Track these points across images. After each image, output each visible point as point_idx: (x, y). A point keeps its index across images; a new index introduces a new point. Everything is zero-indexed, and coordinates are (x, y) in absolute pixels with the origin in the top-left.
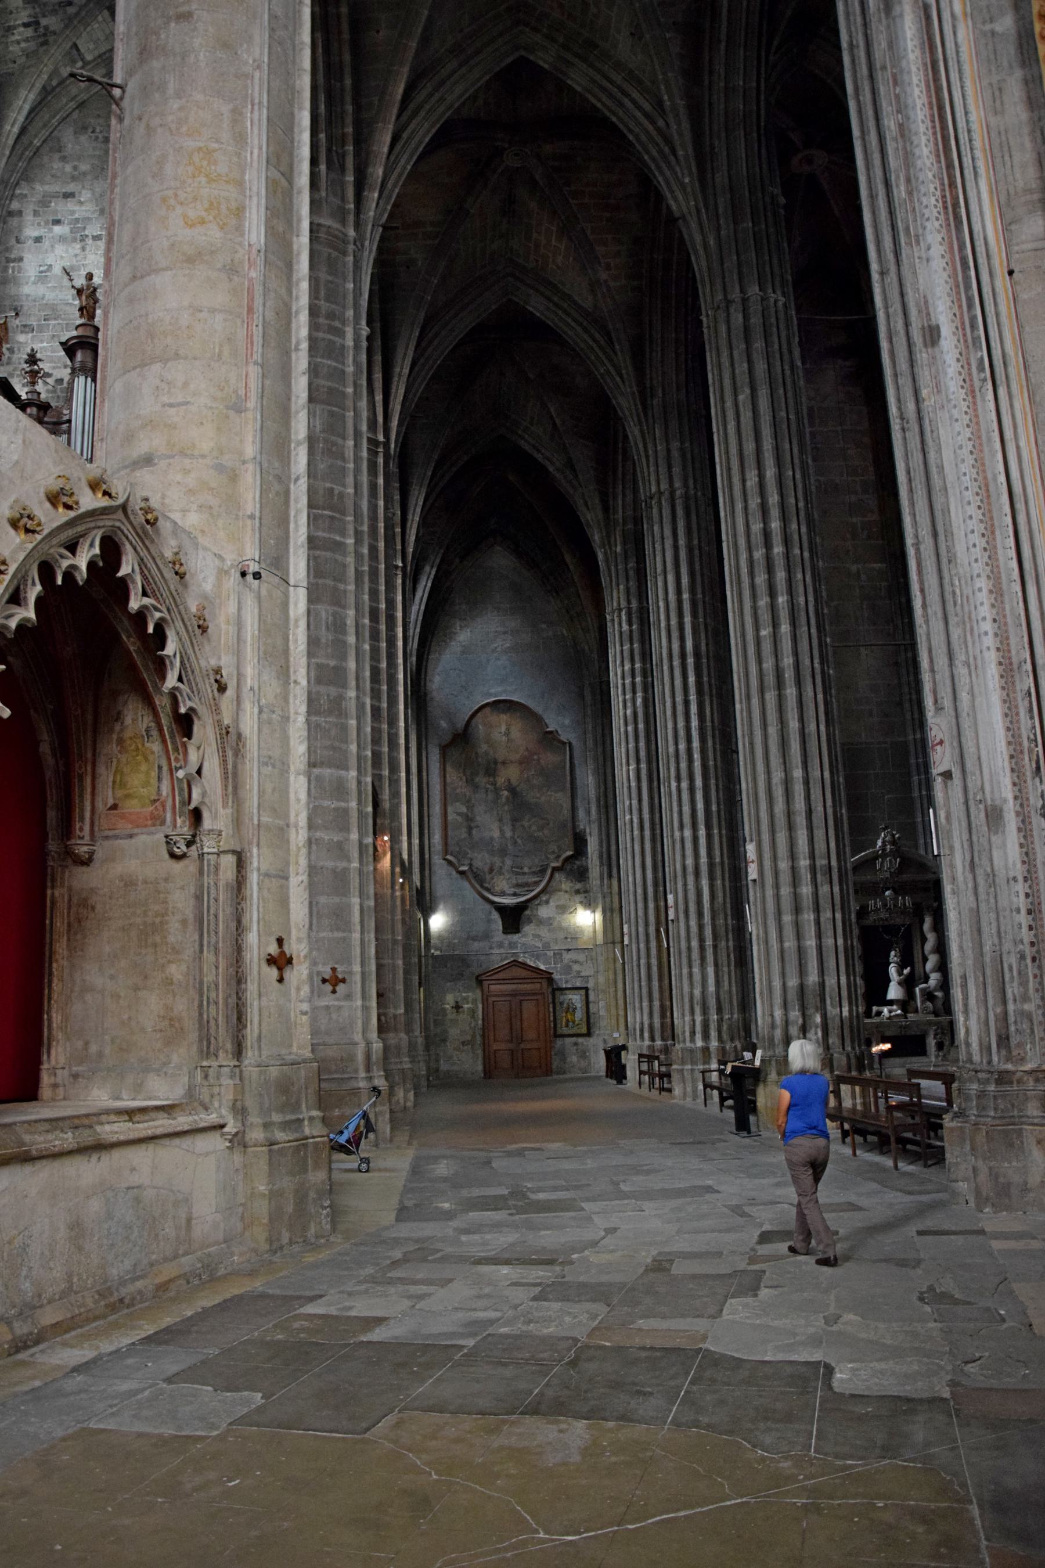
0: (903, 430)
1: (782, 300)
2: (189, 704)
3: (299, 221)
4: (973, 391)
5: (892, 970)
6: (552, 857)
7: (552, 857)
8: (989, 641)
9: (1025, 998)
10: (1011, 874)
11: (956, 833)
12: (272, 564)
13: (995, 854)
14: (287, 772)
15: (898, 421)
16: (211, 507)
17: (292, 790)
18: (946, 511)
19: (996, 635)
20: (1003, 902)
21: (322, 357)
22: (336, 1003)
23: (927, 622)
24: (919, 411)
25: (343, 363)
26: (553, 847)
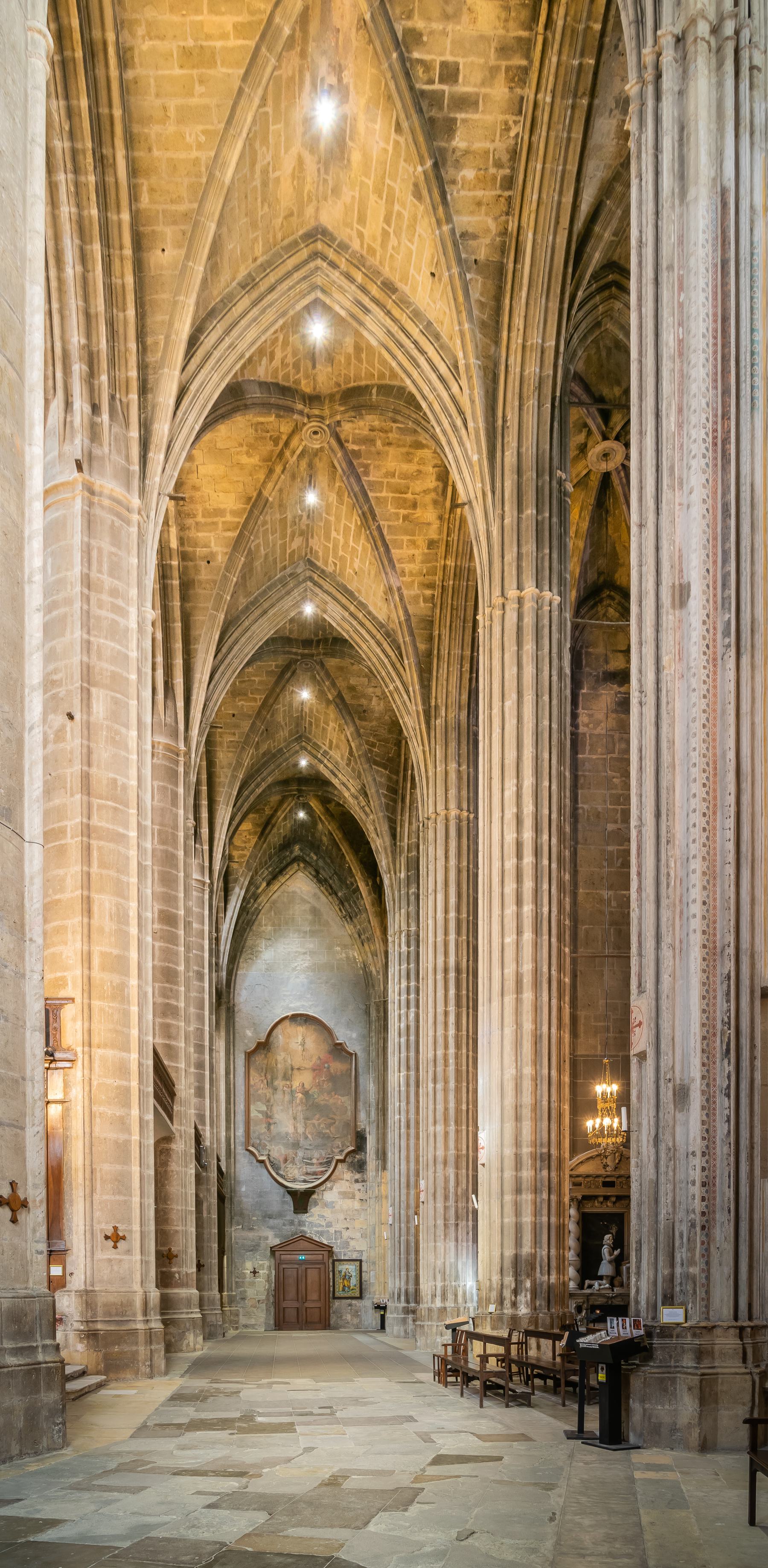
0: (641, 704)
5: (605, 1250)
6: (336, 1151)
7: (336, 1151)
9: (692, 1262)
10: (691, 1149)
11: (644, 1112)
13: (679, 1130)
20: (681, 1175)
21: (106, 638)
22: (118, 1257)
24: (658, 682)
25: (127, 648)
26: (338, 1143)
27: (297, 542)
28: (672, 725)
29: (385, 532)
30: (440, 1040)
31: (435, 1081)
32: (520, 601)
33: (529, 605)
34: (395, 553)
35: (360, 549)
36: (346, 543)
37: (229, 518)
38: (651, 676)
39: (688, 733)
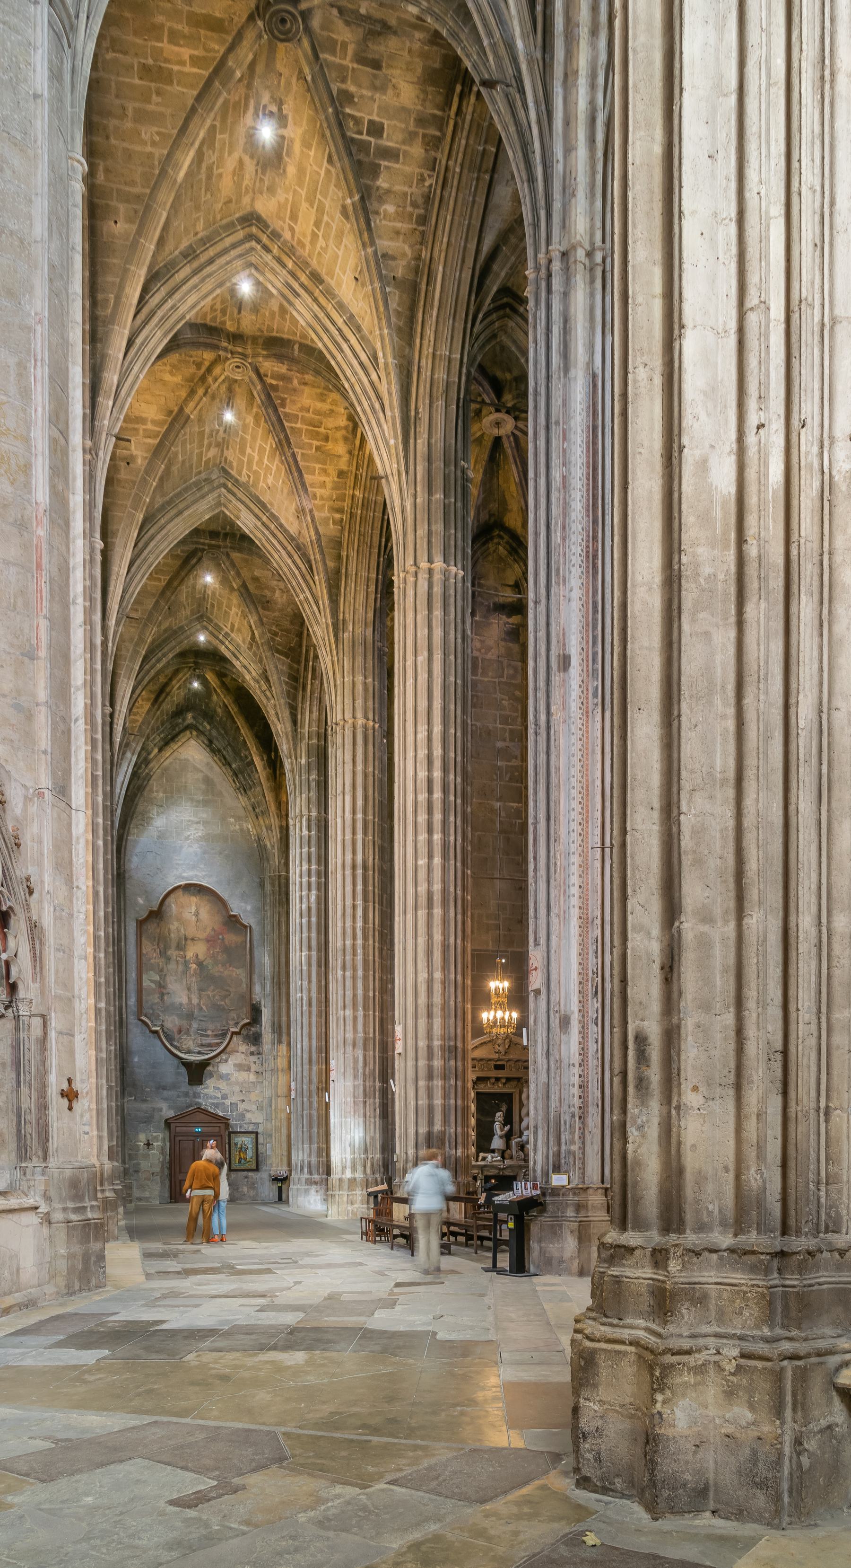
0: (536, 733)
1: (461, 573)
2: (9, 904)
3: (74, 479)
4: (587, 712)
8: (575, 901)
11: (539, 1032)
12: (59, 792)
14: (73, 956)
15: (533, 726)
16: (12, 741)
17: (76, 970)
18: (558, 802)
19: (580, 897)
23: (536, 882)
24: (548, 722)
27: (213, 452)
28: (558, 756)
29: (299, 458)
30: (349, 931)
31: (344, 969)
32: (430, 572)
33: (437, 577)
34: (308, 478)
35: (274, 468)
36: (261, 461)
37: (150, 426)
38: (543, 718)
39: (569, 763)
